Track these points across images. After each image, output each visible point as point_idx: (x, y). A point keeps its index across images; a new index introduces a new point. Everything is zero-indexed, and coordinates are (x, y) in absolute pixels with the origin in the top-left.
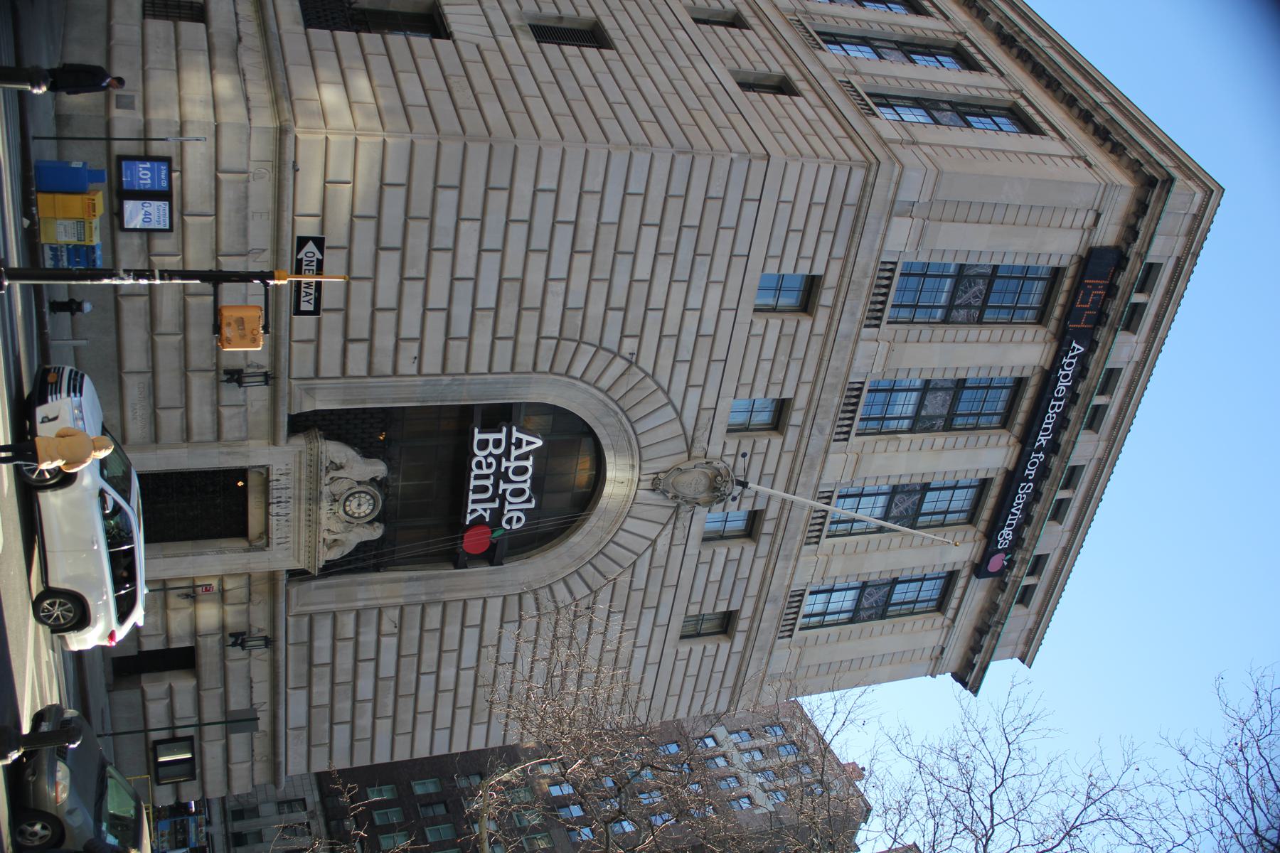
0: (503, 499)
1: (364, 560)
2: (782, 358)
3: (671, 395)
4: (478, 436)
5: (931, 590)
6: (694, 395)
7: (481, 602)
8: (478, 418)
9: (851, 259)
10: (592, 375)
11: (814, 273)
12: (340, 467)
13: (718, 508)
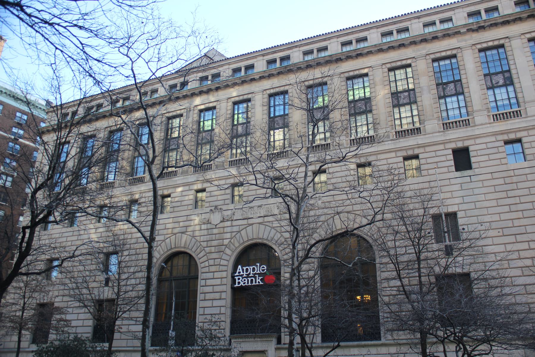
0: (256, 274)
4: (237, 285)
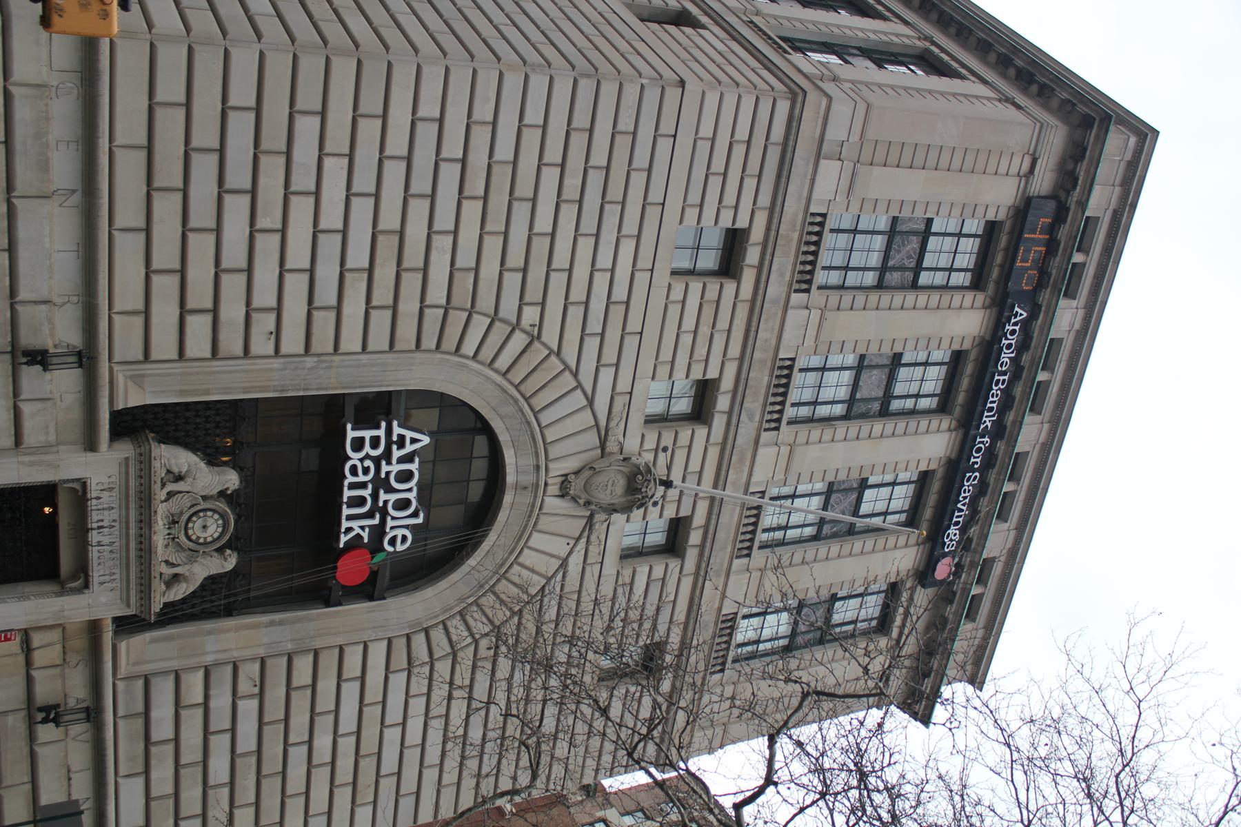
0: (384, 513)
1: (215, 601)
2: (705, 330)
3: (581, 377)
4: (351, 434)
5: (872, 607)
6: (606, 376)
7: (362, 646)
8: (350, 411)
9: (778, 209)
10: (487, 353)
11: (738, 226)
12: (179, 478)
13: (637, 514)
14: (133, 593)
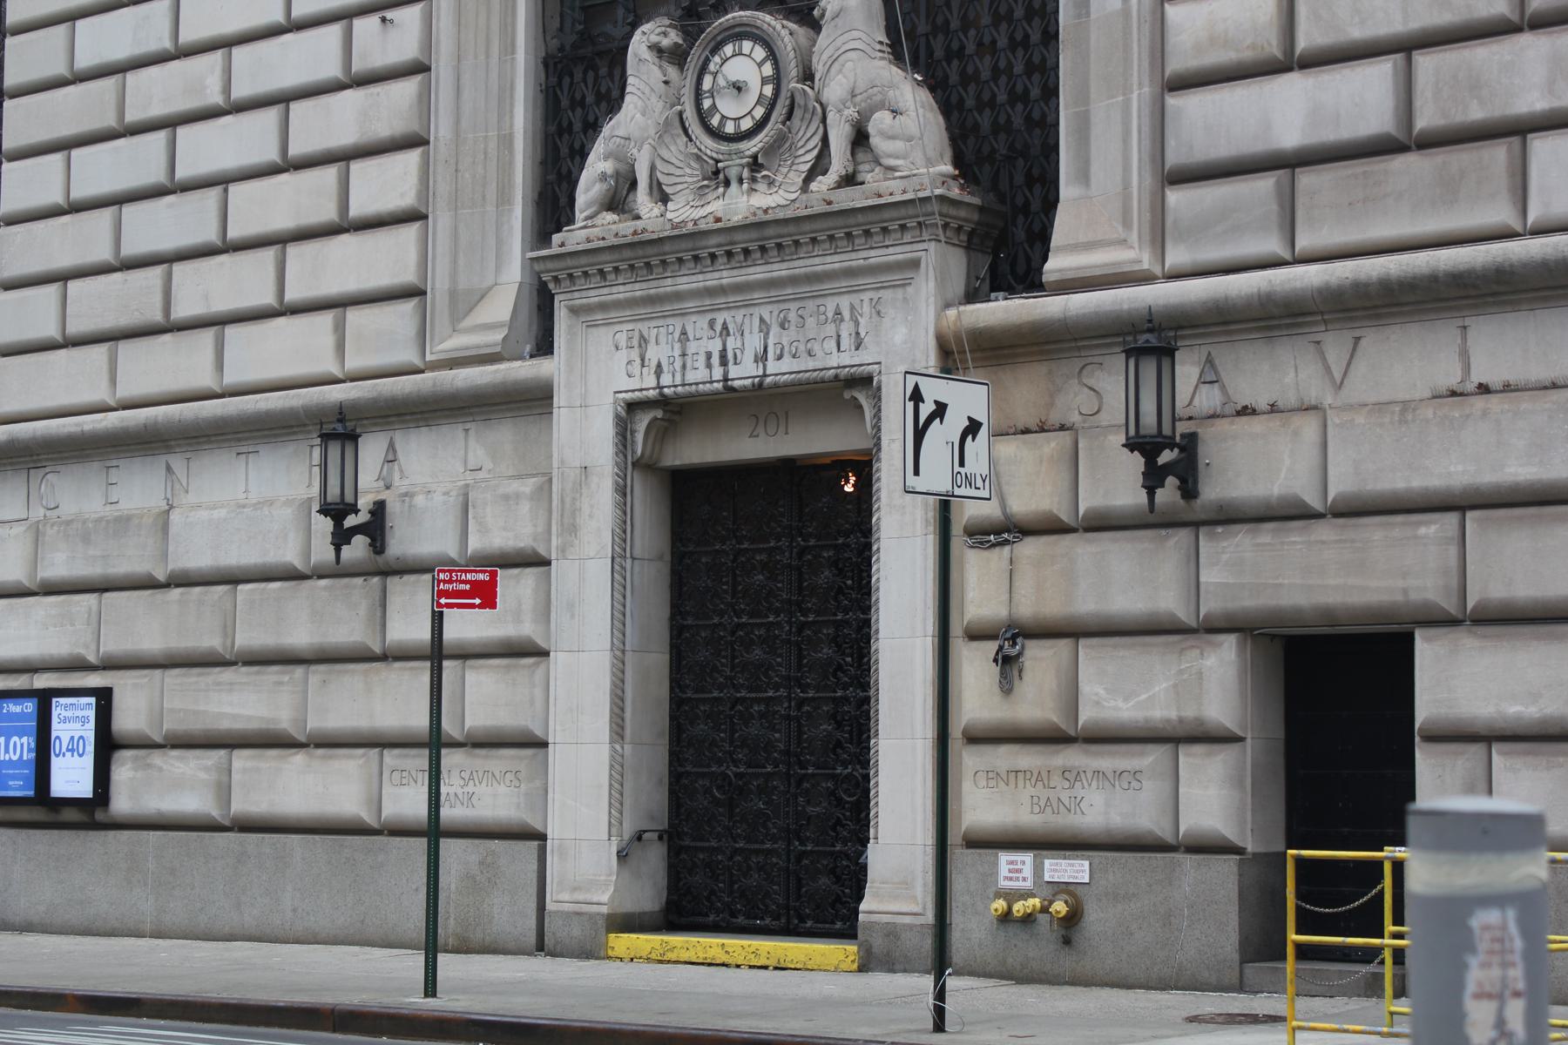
14: (876, 256)
